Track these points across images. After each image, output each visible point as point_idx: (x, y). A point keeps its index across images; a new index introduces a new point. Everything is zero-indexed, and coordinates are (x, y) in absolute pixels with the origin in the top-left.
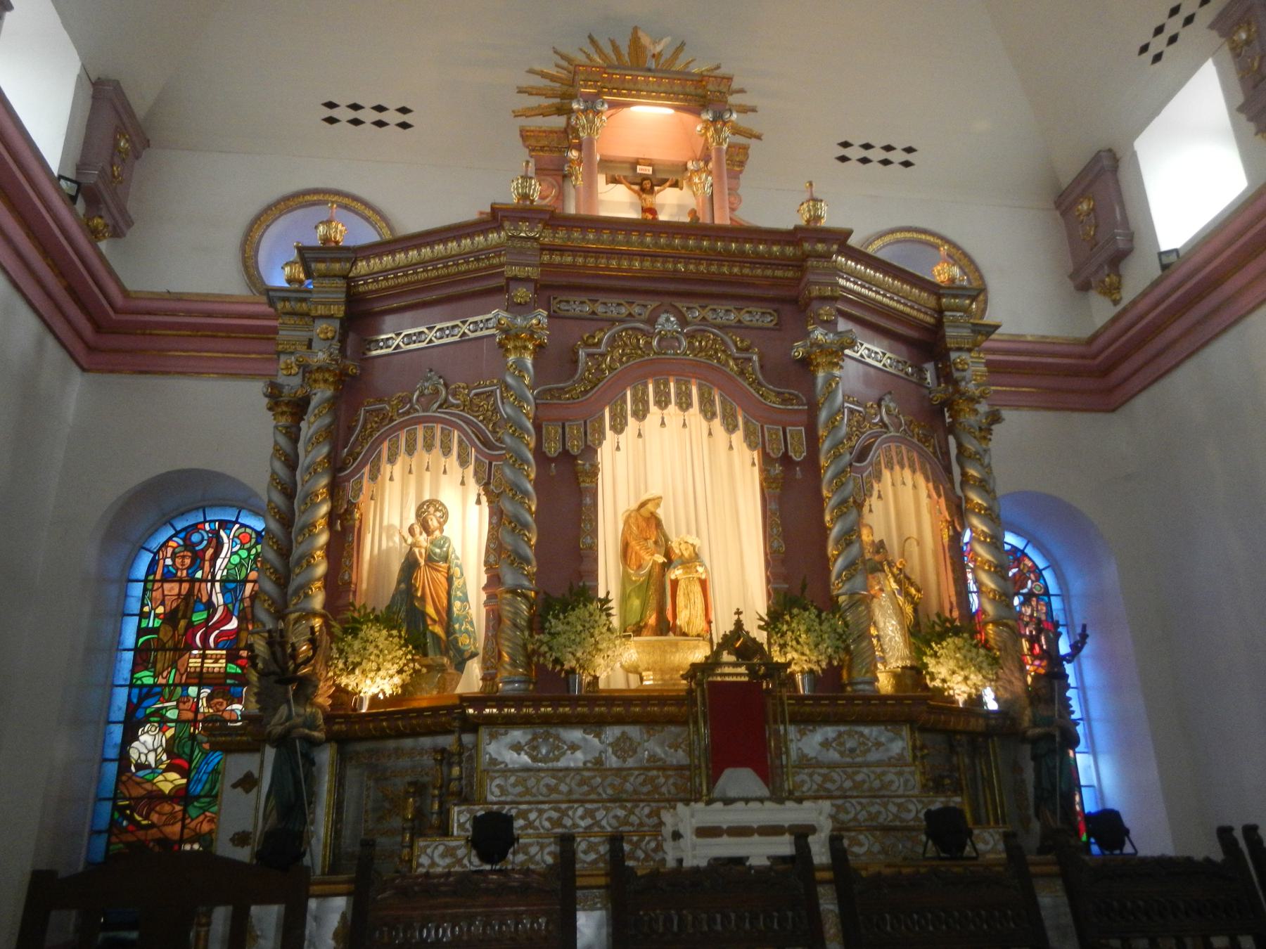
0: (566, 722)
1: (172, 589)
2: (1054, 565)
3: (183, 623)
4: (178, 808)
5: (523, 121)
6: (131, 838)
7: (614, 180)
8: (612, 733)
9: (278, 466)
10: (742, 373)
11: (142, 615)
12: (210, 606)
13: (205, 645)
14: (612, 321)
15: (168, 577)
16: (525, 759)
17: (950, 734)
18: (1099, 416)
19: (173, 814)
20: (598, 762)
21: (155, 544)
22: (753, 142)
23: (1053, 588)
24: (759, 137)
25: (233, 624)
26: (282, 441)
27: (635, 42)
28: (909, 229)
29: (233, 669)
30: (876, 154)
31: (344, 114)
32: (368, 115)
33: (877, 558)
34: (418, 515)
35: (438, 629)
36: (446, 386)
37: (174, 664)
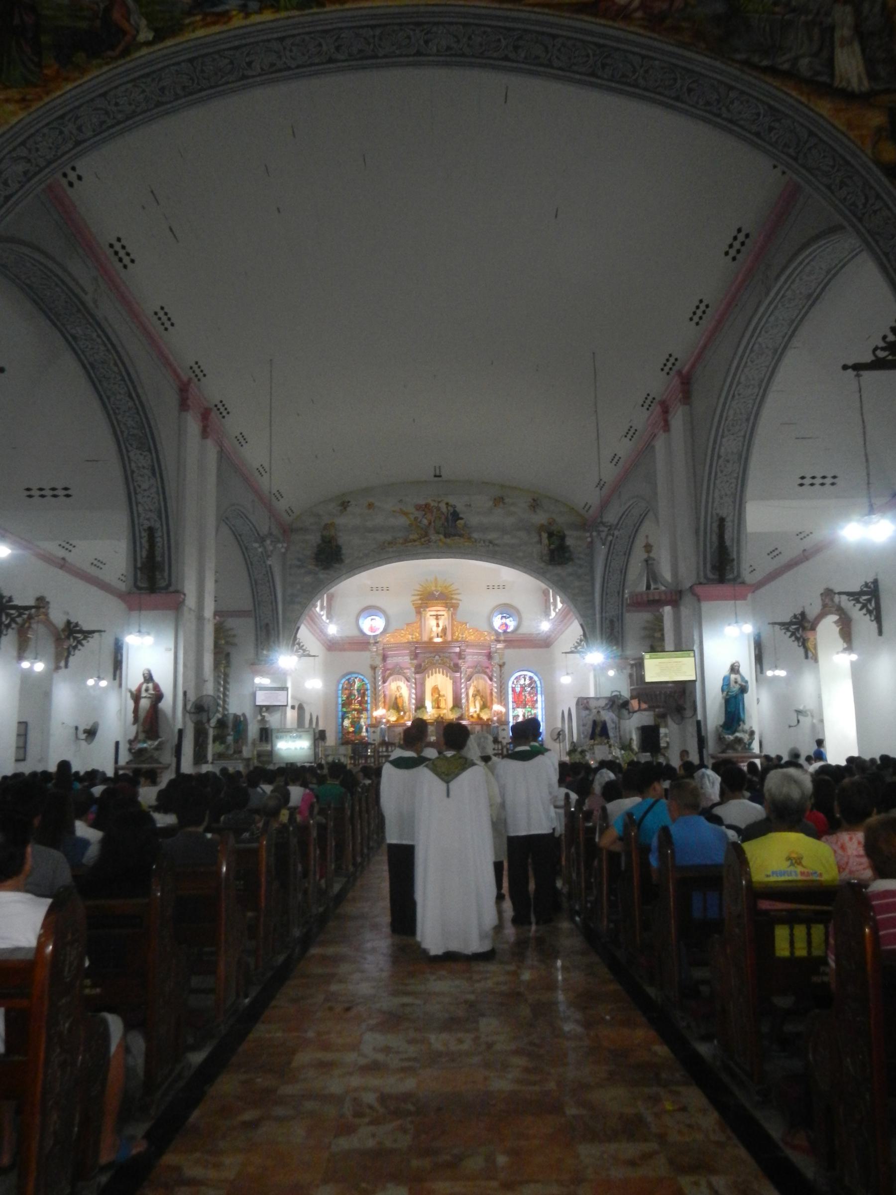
2: (540, 680)
7: (431, 615)
9: (373, 680)
11: (342, 697)
12: (355, 695)
13: (355, 703)
14: (428, 658)
15: (346, 689)
17: (482, 725)
18: (547, 649)
19: (353, 736)
22: (459, 602)
23: (539, 685)
25: (360, 699)
27: (436, 579)
28: (505, 604)
29: (361, 708)
32: (380, 589)
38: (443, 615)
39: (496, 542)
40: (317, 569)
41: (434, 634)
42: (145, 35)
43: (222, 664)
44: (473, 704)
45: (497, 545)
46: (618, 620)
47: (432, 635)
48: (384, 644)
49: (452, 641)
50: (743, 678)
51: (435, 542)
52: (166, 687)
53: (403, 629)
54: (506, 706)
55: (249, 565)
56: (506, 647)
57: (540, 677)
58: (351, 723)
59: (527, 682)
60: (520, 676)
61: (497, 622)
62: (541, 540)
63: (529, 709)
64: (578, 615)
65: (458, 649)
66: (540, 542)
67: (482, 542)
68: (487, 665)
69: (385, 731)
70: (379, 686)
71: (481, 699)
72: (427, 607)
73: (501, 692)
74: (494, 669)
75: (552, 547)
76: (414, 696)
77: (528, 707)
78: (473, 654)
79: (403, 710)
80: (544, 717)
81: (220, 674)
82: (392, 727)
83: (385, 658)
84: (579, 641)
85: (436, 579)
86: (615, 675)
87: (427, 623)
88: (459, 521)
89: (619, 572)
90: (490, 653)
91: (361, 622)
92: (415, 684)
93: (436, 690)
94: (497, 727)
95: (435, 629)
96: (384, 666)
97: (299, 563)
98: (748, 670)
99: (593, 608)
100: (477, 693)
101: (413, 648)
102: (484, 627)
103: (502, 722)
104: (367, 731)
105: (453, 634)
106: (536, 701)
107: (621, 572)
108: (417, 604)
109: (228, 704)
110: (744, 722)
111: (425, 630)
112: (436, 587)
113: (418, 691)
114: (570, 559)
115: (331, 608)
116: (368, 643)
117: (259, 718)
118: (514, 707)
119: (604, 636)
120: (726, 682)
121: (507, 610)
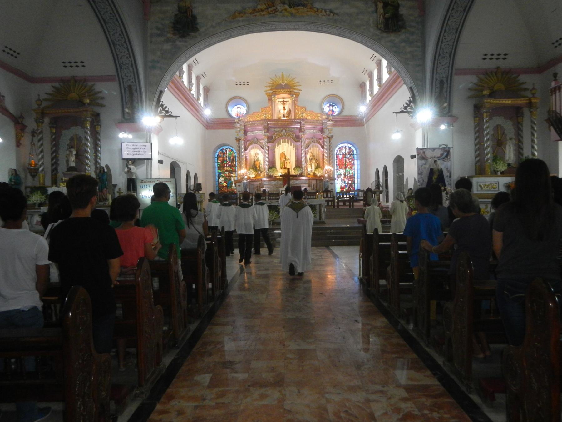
0: (272, 180)
1: (221, 158)
2: (356, 149)
3: (223, 163)
4: (226, 188)
5: (266, 92)
6: (221, 192)
7: (279, 102)
8: (276, 181)
9: (238, 148)
10: (293, 137)
11: (218, 162)
12: (227, 161)
14: (277, 131)
15: (220, 157)
16: (268, 184)
17: (316, 180)
20: (275, 184)
21: (218, 151)
23: (355, 153)
24: (301, 90)
25: (230, 163)
26: (238, 145)
27: (283, 75)
29: (231, 169)
30: (326, 82)
31: (238, 84)
32: (242, 84)
33: (313, 158)
34: (255, 154)
35: (258, 169)
36: (257, 140)
37: (223, 169)
38: (288, 101)
39: (336, 11)
40: (174, 37)
41: (282, 115)
43: (88, 120)
44: (310, 165)
45: (337, 14)
46: (447, 81)
47: (280, 116)
48: (245, 122)
49: (295, 119)
51: (281, 12)
53: (259, 112)
54: (333, 167)
55: (103, 23)
56: (334, 125)
57: (357, 148)
58: (224, 180)
59: (347, 151)
60: (343, 146)
61: (327, 109)
62: (377, 9)
63: (348, 170)
64: (408, 80)
65: (299, 125)
66: (376, 11)
67: (323, 11)
68: (320, 137)
69: (247, 185)
70: (242, 153)
71: (316, 162)
72: (276, 95)
73: (330, 157)
74: (325, 140)
75: (387, 15)
76: (267, 159)
77: (347, 168)
79: (260, 170)
80: (359, 175)
81: (86, 130)
82: (251, 181)
83: (246, 132)
84: (408, 102)
85: (283, 75)
86: (445, 130)
87: (276, 107)
89: (454, 31)
90: (322, 129)
91: (230, 109)
92: (268, 150)
93: (283, 155)
94: (328, 181)
95: (282, 111)
96: (246, 139)
97: (159, 32)
99: (424, 71)
100: (313, 158)
101: (266, 124)
102: (317, 110)
103: (331, 178)
104: (235, 186)
106: (354, 164)
107: (456, 32)
108: (270, 93)
109: (100, 160)
111: (275, 110)
112: (283, 80)
113: (270, 155)
114: (403, 27)
115: (207, 98)
116: (235, 123)
117: (126, 170)
118: (338, 168)
119: (433, 96)
121: (334, 99)
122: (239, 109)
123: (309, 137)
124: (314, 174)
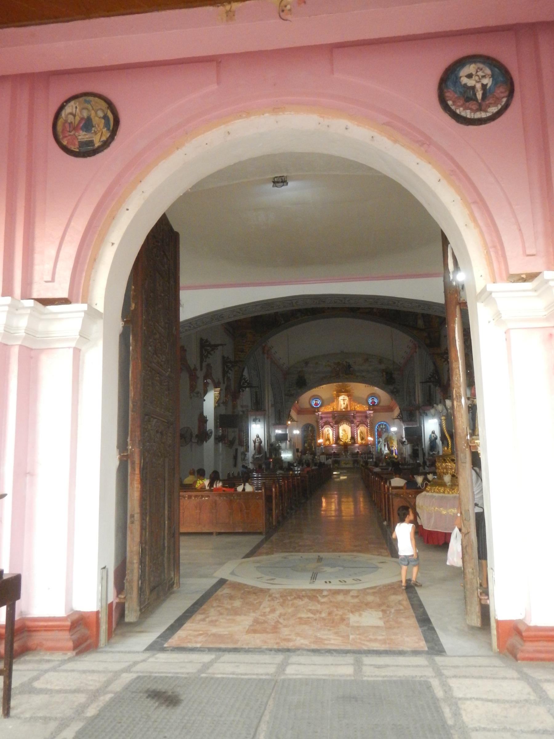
42: (283, 322)
47: (342, 408)
49: (350, 411)
50: (436, 435)
52: (263, 440)
59: (384, 427)
66: (383, 376)
76: (334, 434)
78: (359, 416)
82: (326, 447)
88: (351, 369)
98: (438, 433)
100: (361, 433)
105: (350, 407)
110: (436, 449)
120: (431, 436)
122: (316, 401)
123: (359, 421)
124: (362, 443)
